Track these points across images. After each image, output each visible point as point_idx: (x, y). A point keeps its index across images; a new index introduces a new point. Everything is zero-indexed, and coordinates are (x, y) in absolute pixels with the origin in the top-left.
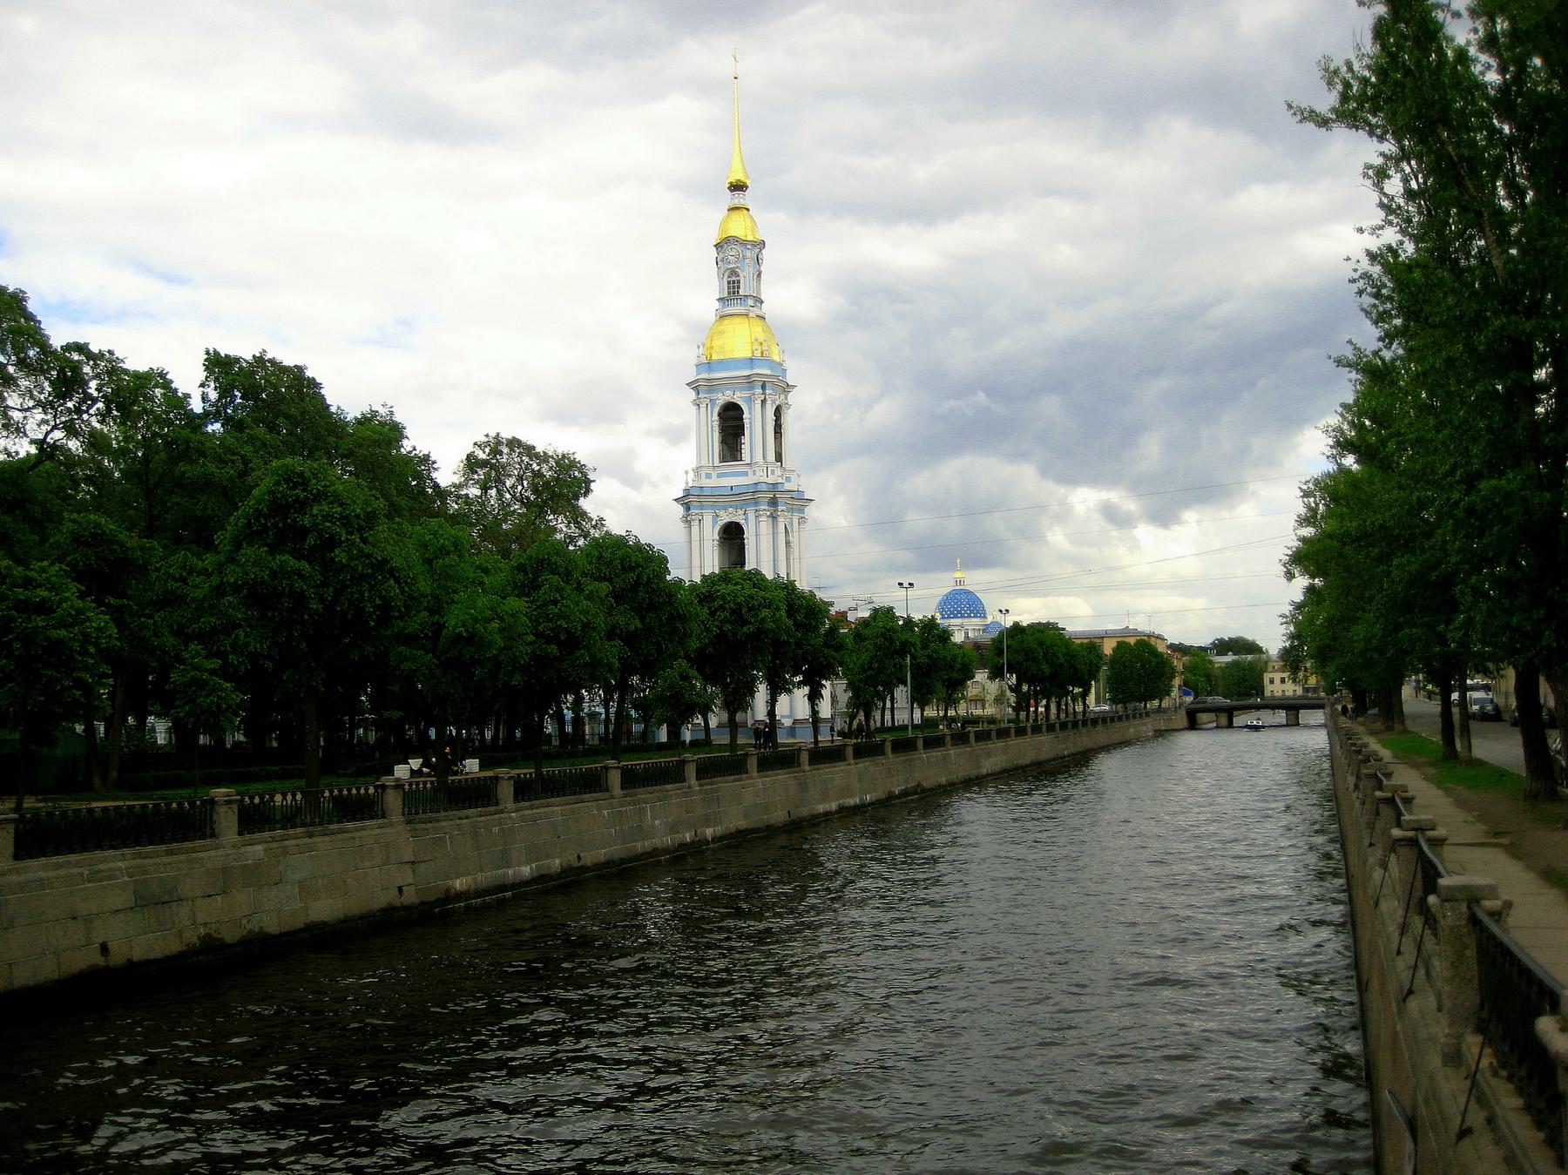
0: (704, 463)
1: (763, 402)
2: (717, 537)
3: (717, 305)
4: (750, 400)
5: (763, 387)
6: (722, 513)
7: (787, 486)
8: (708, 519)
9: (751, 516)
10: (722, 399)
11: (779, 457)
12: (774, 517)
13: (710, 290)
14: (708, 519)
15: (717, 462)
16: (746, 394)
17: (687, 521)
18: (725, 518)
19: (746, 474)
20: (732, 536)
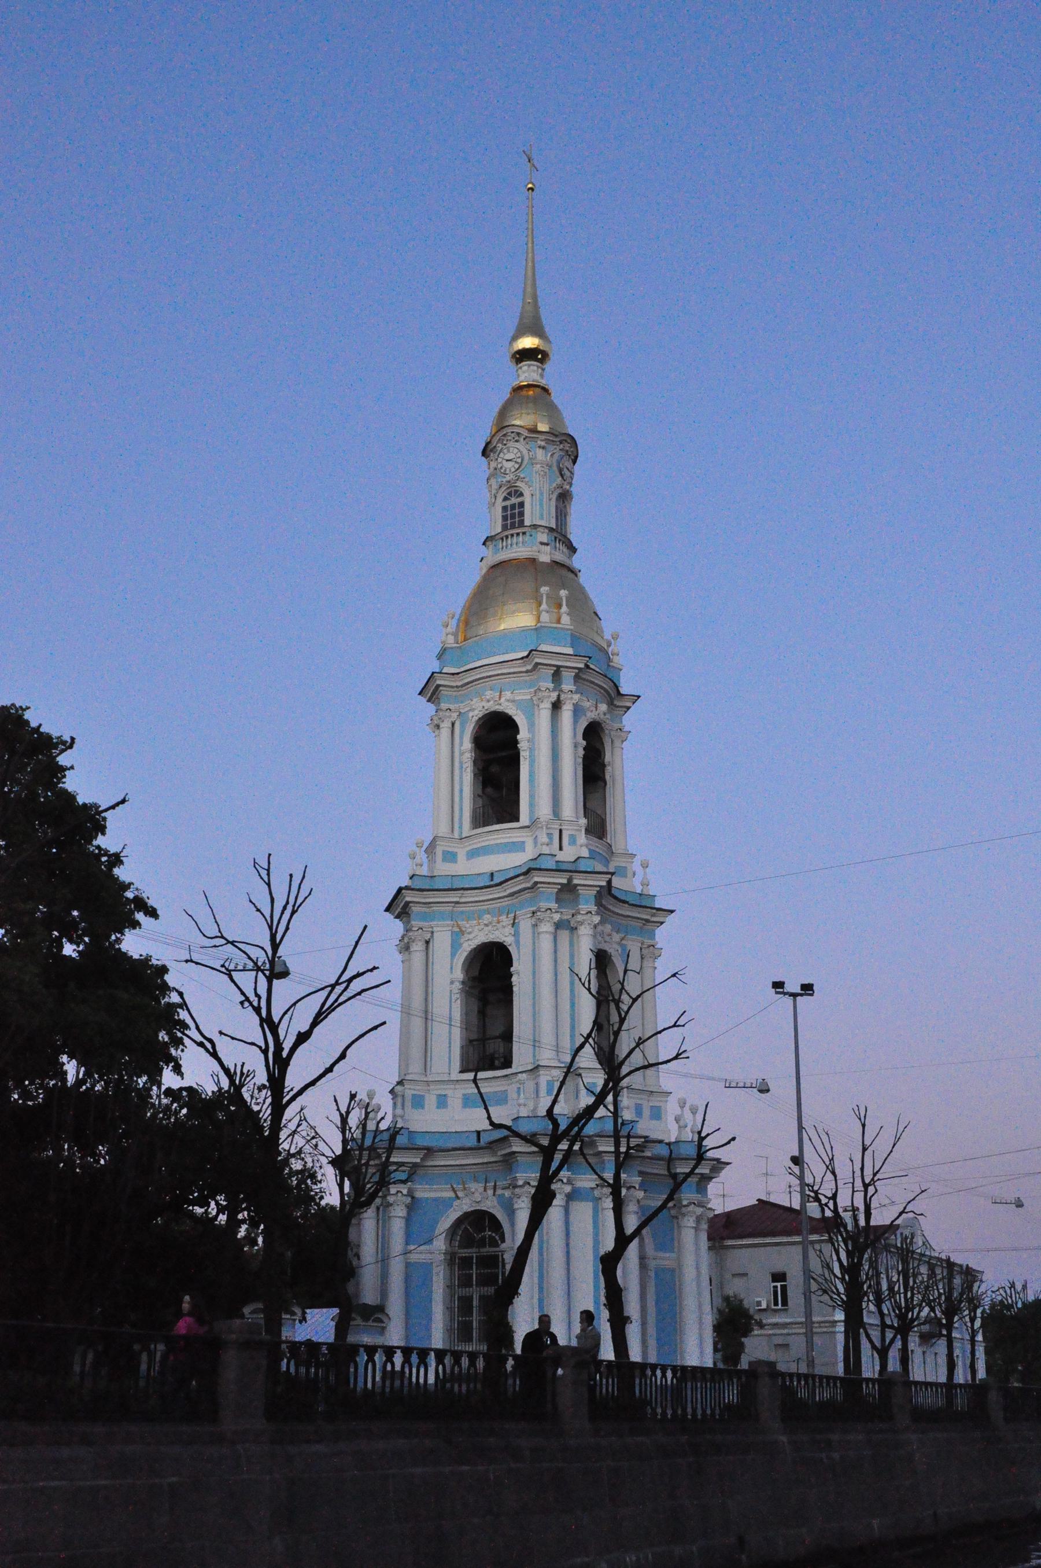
1: (556, 706)
2: (459, 975)
10: (478, 707)
19: (519, 847)
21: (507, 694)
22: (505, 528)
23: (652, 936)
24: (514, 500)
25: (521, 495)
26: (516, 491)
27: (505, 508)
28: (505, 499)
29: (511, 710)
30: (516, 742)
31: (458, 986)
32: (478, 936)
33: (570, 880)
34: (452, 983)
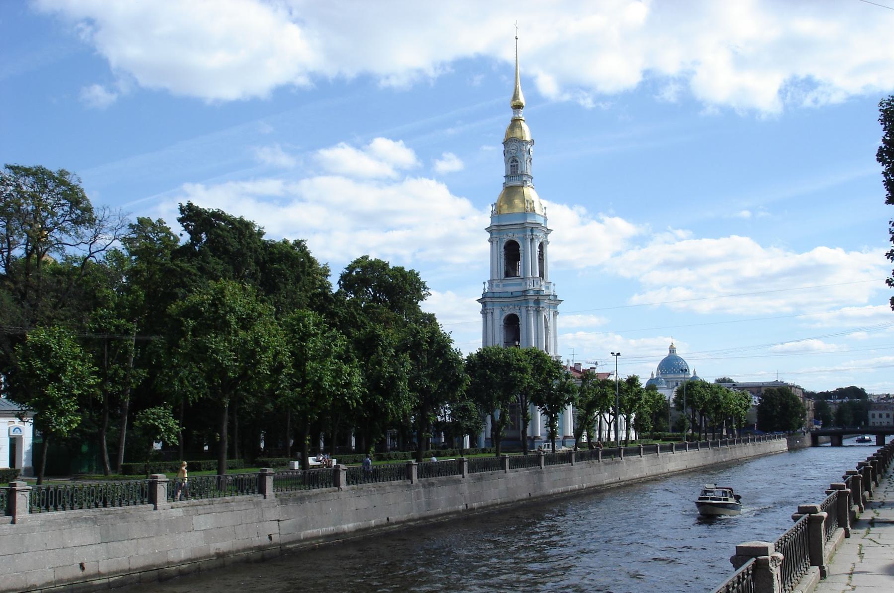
0: (495, 277)
2: (502, 323)
3: (504, 180)
4: (524, 239)
6: (505, 309)
7: (546, 292)
8: (497, 312)
9: (524, 310)
10: (506, 239)
12: (538, 312)
13: (500, 170)
14: (497, 312)
16: (521, 235)
17: (484, 312)
18: (508, 312)
19: (520, 284)
20: (512, 324)
21: (516, 235)
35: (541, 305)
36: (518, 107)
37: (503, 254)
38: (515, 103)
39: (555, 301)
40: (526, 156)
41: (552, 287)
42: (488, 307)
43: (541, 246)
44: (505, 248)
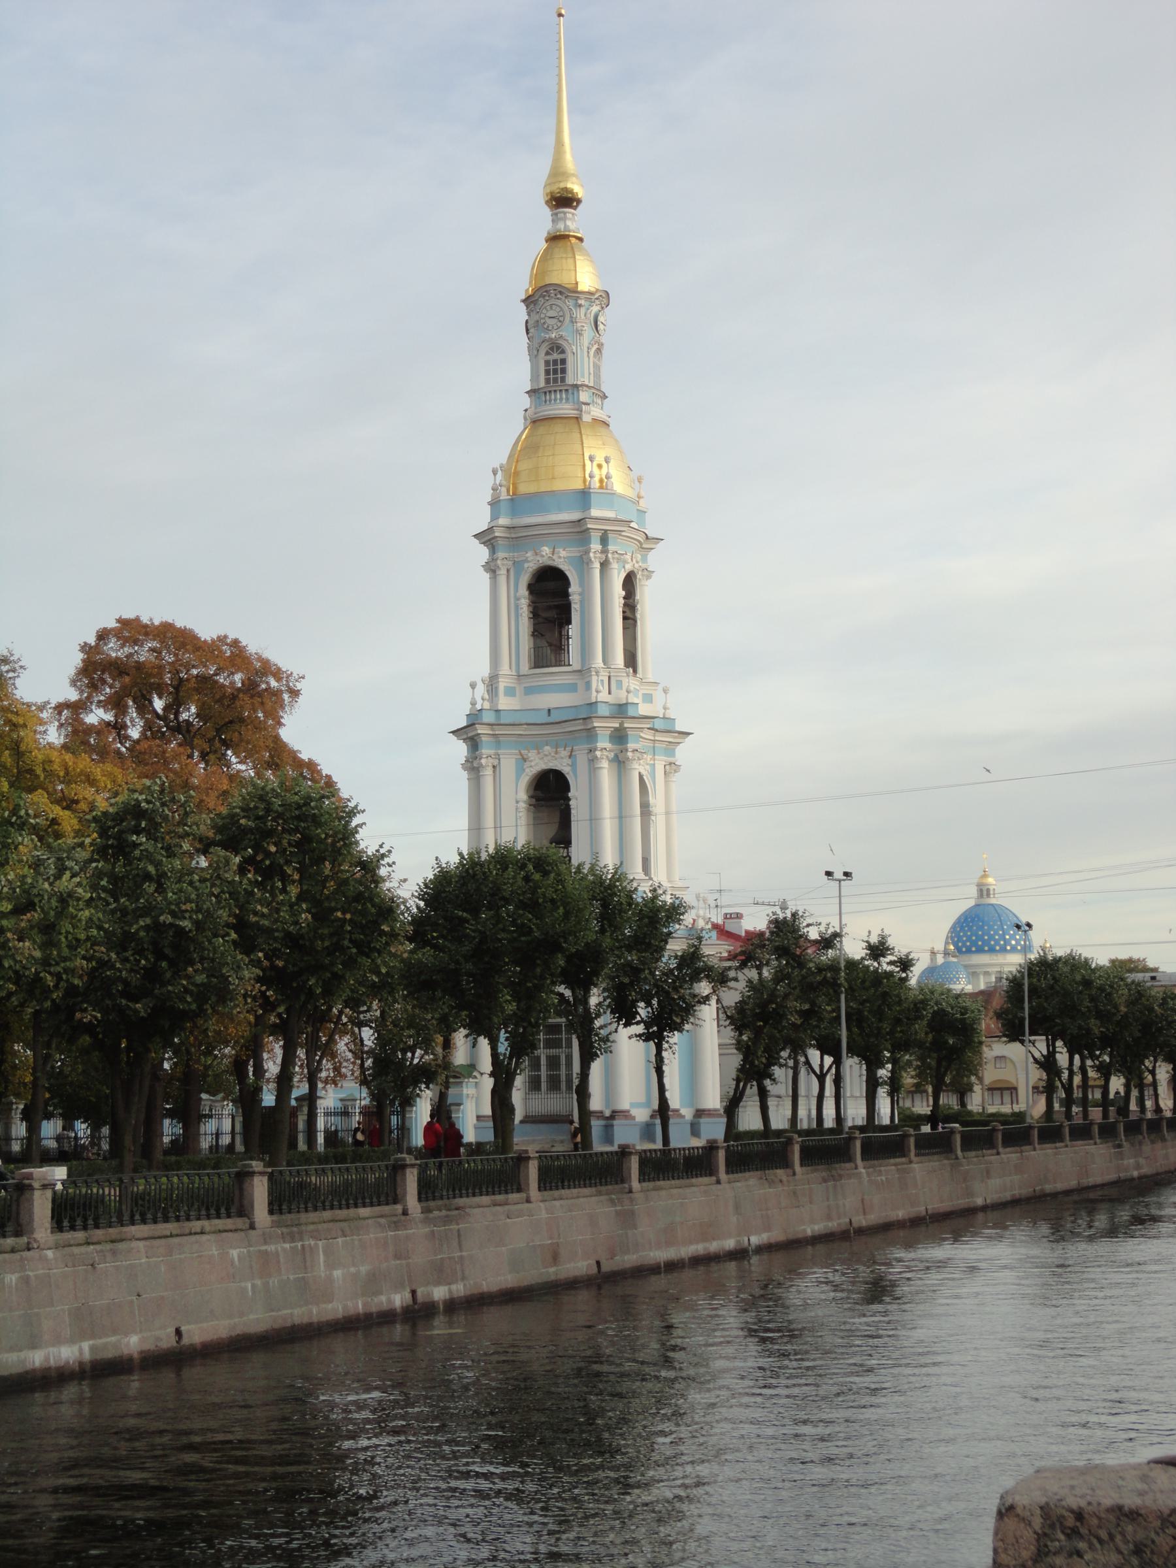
1: (604, 565)
2: (523, 796)
3: (526, 402)
4: (583, 562)
5: (604, 540)
6: (532, 754)
7: (644, 709)
8: (508, 765)
9: (582, 759)
11: (631, 660)
12: (620, 763)
13: (517, 370)
15: (525, 668)
17: (473, 766)
19: (573, 688)
20: (550, 791)
22: (547, 381)
23: (674, 756)
24: (556, 356)
25: (563, 352)
26: (558, 347)
27: (547, 363)
28: (547, 353)
29: (564, 567)
30: (566, 595)
31: (522, 805)
32: (538, 763)
33: (621, 724)
34: (517, 802)
35: (631, 746)
36: (563, 201)
37: (524, 603)
38: (555, 188)
39: (670, 734)
40: (588, 333)
41: (658, 696)
42: (485, 751)
43: (629, 582)
44: (531, 588)
